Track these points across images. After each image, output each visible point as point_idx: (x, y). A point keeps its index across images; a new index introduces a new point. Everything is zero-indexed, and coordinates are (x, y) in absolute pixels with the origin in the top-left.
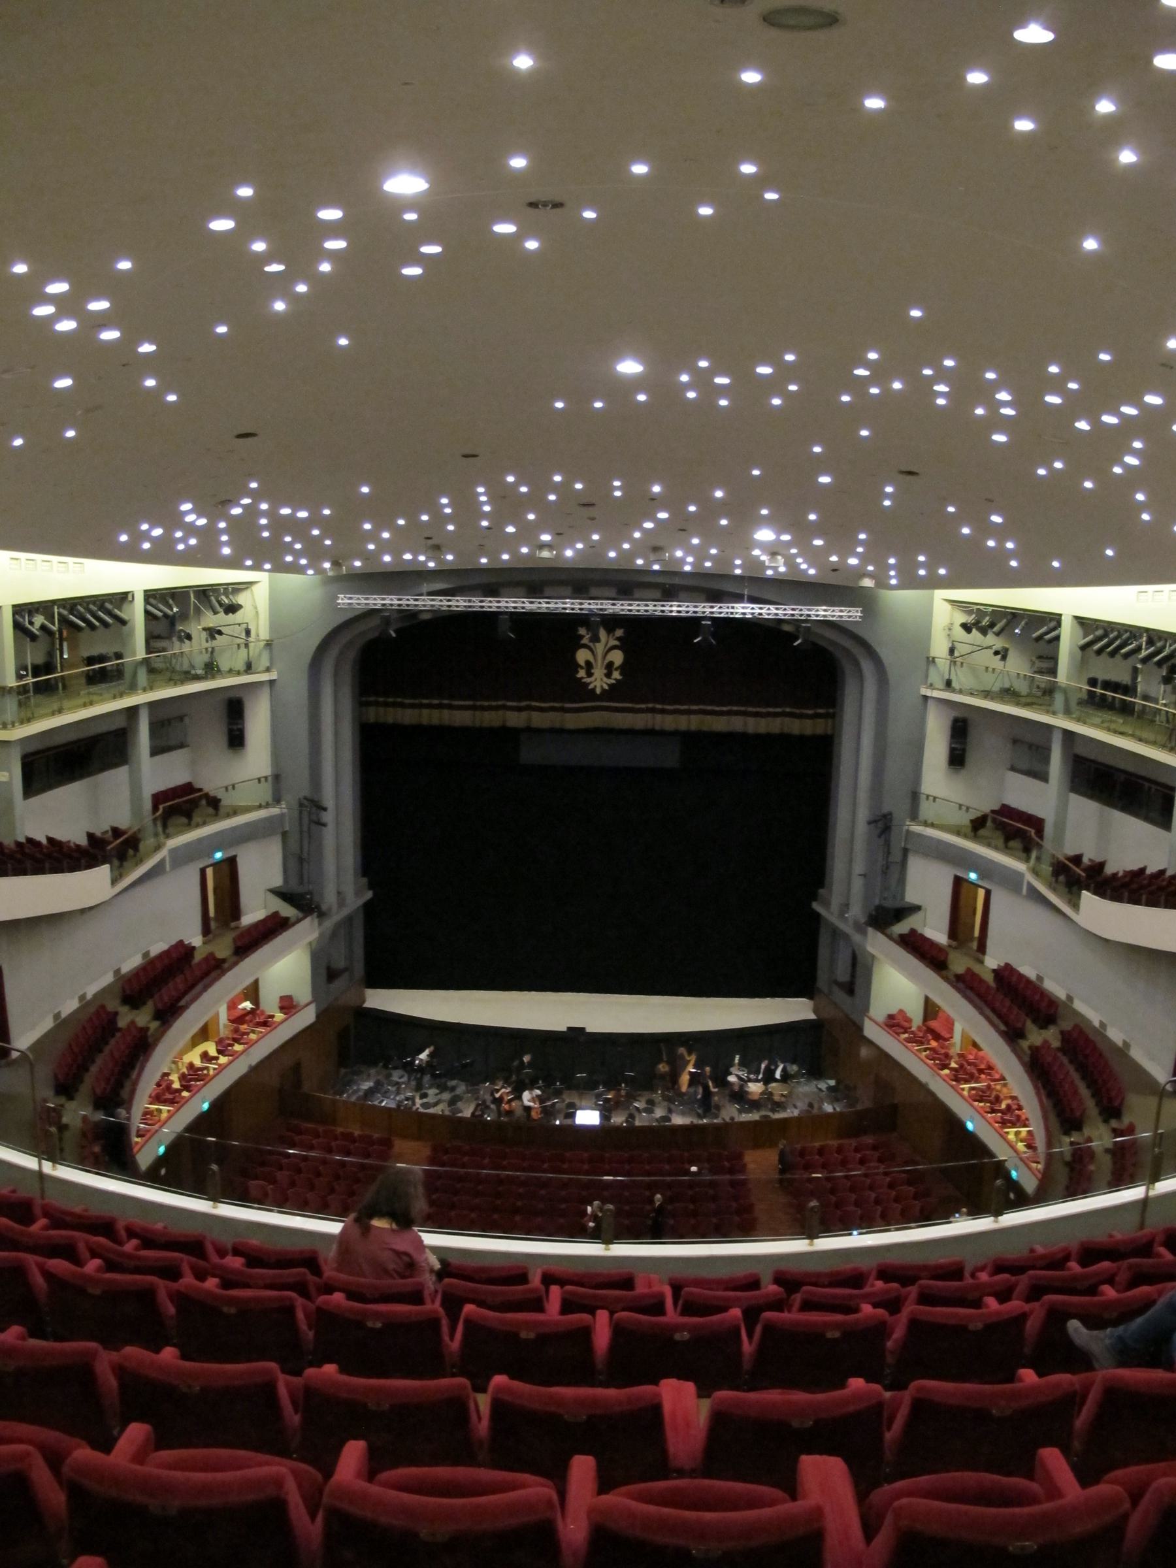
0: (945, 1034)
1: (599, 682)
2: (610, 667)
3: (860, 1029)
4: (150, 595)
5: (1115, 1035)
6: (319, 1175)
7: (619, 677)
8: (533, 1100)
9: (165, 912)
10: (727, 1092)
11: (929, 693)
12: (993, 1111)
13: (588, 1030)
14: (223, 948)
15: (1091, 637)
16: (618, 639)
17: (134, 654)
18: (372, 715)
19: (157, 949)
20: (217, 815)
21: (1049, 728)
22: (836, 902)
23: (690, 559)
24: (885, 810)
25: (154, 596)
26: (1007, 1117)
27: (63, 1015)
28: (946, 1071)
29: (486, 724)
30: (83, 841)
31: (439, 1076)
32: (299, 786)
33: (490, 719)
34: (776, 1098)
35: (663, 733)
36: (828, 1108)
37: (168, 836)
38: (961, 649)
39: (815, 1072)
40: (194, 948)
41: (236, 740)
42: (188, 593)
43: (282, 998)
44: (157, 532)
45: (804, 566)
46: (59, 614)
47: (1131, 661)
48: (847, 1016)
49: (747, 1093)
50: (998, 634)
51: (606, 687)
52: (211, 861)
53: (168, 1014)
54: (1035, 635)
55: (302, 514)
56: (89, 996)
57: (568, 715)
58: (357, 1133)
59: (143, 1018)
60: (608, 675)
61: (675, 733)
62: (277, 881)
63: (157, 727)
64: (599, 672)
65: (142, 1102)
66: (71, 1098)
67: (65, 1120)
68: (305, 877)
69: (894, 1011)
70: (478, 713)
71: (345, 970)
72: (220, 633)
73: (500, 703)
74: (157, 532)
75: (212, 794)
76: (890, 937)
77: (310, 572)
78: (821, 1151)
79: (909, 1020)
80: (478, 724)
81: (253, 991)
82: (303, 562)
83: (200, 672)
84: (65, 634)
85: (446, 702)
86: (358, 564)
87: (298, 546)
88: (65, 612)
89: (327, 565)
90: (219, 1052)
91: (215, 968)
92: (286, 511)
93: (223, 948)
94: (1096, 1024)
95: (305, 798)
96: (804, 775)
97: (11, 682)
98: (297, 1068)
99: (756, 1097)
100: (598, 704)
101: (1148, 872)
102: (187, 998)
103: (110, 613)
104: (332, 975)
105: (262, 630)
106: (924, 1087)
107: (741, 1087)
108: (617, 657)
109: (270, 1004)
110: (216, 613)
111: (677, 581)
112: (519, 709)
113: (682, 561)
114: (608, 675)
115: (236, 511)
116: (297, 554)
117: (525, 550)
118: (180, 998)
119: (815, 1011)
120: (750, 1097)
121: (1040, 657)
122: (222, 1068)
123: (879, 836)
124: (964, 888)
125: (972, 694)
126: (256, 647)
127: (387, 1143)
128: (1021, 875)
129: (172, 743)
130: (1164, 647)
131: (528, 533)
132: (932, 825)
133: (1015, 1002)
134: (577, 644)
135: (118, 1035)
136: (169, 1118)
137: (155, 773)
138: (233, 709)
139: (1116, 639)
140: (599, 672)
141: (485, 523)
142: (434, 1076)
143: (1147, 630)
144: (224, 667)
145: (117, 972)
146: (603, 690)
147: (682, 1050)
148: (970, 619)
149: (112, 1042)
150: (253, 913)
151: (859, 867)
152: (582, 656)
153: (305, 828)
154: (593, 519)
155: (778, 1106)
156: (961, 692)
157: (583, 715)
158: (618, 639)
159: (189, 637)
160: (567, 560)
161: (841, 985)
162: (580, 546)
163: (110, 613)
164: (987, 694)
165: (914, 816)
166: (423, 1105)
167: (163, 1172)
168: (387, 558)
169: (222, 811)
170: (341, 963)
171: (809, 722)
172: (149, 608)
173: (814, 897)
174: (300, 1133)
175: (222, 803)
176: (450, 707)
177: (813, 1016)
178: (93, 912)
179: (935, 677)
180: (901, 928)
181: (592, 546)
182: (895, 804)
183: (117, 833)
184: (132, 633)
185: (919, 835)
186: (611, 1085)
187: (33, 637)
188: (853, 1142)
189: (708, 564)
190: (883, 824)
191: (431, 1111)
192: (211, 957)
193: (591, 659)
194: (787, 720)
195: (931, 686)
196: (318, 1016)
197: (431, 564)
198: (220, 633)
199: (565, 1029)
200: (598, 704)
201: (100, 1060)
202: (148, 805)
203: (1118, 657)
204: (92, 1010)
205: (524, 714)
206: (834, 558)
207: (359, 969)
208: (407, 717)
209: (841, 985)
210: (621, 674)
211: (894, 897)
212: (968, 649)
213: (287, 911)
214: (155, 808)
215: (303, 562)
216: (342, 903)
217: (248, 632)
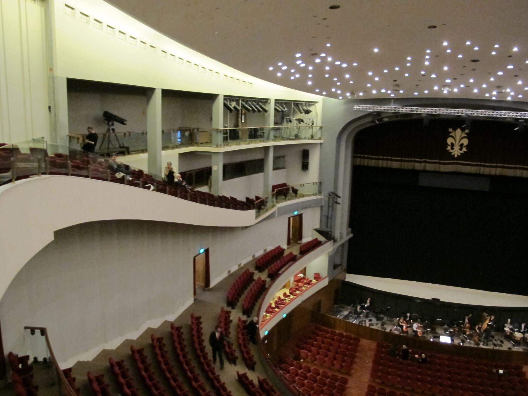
1: (456, 152)
4: (277, 102)
6: (329, 350)
9: (273, 235)
13: (441, 300)
14: (295, 250)
16: (466, 134)
17: (269, 125)
18: (358, 162)
19: (270, 248)
20: (296, 196)
23: (512, 94)
25: (278, 103)
27: (232, 272)
29: (406, 168)
30: (244, 200)
31: (377, 313)
32: (329, 188)
35: (483, 176)
37: (277, 202)
40: (284, 249)
41: (305, 167)
42: (291, 103)
43: (315, 274)
44: (284, 68)
46: (242, 104)
49: (515, 337)
51: (459, 154)
52: (293, 215)
53: (274, 276)
55: (344, 65)
56: (242, 265)
57: (442, 166)
58: (345, 334)
59: (264, 276)
60: (461, 149)
61: (490, 176)
62: (318, 226)
63: (276, 159)
64: (457, 147)
65: (263, 313)
66: (233, 308)
67: (231, 318)
68: (329, 225)
70: (403, 163)
71: (340, 265)
72: (302, 121)
73: (413, 159)
74: (284, 68)
75: (295, 187)
77: (341, 98)
80: (402, 167)
81: (304, 271)
82: (339, 92)
84: (243, 112)
85: (389, 158)
86: (361, 94)
87: (338, 84)
88: (244, 103)
89: (348, 94)
90: (290, 293)
91: (293, 259)
92: (338, 63)
93: (295, 250)
95: (332, 192)
97: (221, 127)
98: (319, 303)
99: (519, 339)
100: (455, 161)
102: (283, 270)
103: (261, 107)
104: (335, 267)
105: (318, 122)
107: (511, 333)
108: (465, 142)
109: (310, 275)
110: (301, 113)
111: (503, 105)
112: (420, 162)
113: (508, 94)
114: (461, 149)
115: (318, 61)
116: (337, 88)
117: (436, 88)
118: (279, 269)
120: (516, 339)
122: (292, 300)
126: (316, 129)
127: (359, 341)
129: (281, 166)
131: (442, 76)
134: (448, 135)
135: (254, 282)
136: (270, 320)
137: (272, 177)
138: (305, 154)
140: (457, 147)
141: (423, 73)
144: (303, 137)
145: (254, 256)
146: (458, 156)
147: (485, 314)
149: (251, 285)
150: (308, 237)
152: (450, 141)
153: (331, 205)
154: (474, 70)
159: (290, 121)
160: (456, 93)
162: (462, 86)
163: (261, 107)
166: (370, 325)
167: (266, 342)
168: (374, 92)
169: (298, 195)
170: (338, 262)
172: (276, 107)
174: (321, 331)
175: (298, 192)
176: (392, 160)
178: (244, 231)
183: (257, 198)
184: (269, 116)
186: (451, 325)
187: (231, 110)
189: (520, 96)
191: (373, 327)
192: (291, 254)
193: (454, 142)
196: (330, 282)
197: (392, 95)
198: (302, 121)
199: (431, 299)
200: (455, 161)
201: (246, 292)
202: (270, 189)
204: (244, 271)
205: (423, 164)
207: (345, 266)
208: (373, 163)
210: (466, 149)
213: (321, 238)
214: (273, 190)
215: (339, 92)
216: (341, 238)
217: (313, 124)
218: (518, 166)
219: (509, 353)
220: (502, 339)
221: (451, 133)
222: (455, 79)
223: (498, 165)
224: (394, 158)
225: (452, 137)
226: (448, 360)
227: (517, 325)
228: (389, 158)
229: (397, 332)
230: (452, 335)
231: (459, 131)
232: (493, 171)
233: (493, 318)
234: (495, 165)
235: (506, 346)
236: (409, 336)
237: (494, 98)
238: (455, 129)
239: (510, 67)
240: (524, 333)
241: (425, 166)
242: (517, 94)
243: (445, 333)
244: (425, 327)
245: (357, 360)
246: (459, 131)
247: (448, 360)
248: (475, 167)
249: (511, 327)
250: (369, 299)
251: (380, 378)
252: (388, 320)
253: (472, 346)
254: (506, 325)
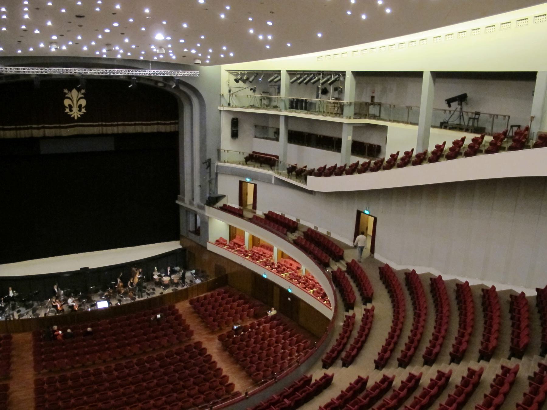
0: (241, 243)
1: (76, 114)
2: (80, 107)
3: (206, 248)
5: (322, 231)
7: (85, 111)
8: (73, 302)
10: (153, 283)
11: (222, 109)
12: (272, 269)
13: (90, 268)
15: (295, 78)
16: (82, 94)
21: (278, 116)
22: (187, 198)
23: (121, 51)
24: (208, 158)
26: (280, 270)
28: (248, 257)
33: (24, 134)
34: (176, 281)
35: (106, 135)
36: (198, 281)
38: (233, 90)
39: (186, 268)
45: (171, 55)
47: (315, 85)
48: (198, 244)
49: (163, 281)
50: (250, 82)
51: (79, 116)
54: (269, 80)
57: (62, 130)
60: (80, 111)
61: (113, 135)
64: (75, 109)
69: (218, 238)
70: (18, 131)
73: (29, 126)
76: (217, 209)
78: (205, 298)
79: (226, 241)
80: (19, 137)
96: (169, 148)
99: (167, 282)
100: (76, 124)
101: (327, 167)
106: (240, 266)
107: (160, 279)
108: (83, 102)
111: (115, 63)
112: (38, 128)
113: (117, 52)
114: (80, 111)
117: (42, 45)
119: (181, 244)
121: (264, 92)
123: (207, 168)
124: (243, 184)
125: (241, 107)
127: (10, 338)
128: (271, 176)
130: (331, 77)
132: (228, 162)
133: (277, 223)
134: (64, 97)
139: (306, 78)
140: (75, 109)
142: (21, 301)
143: (323, 71)
146: (78, 117)
147: (134, 269)
148: (239, 77)
151: (197, 183)
152: (67, 102)
154: (81, 26)
155: (177, 284)
156: (236, 107)
157: (69, 130)
160: (64, 51)
161: (192, 232)
164: (248, 107)
165: (219, 159)
166: (19, 316)
171: (168, 127)
173: (177, 199)
177: (181, 247)
179: (223, 102)
180: (220, 204)
181: (77, 43)
182: (211, 154)
185: (222, 167)
186: (105, 289)
188: (216, 292)
189: (129, 54)
190: (207, 164)
193: (72, 104)
194: (160, 126)
195: (223, 106)
200: (76, 124)
203: (309, 84)
205: (42, 130)
206: (186, 50)
209: (192, 232)
210: (85, 110)
211: (214, 193)
212: (238, 89)
218: (137, 122)
219: (162, 297)
220: (154, 287)
221: (67, 94)
222: (62, 35)
223: (120, 123)
224: (6, 127)
226: (110, 323)
227: (163, 270)
229: (51, 314)
230: (108, 299)
231: (74, 92)
232: (115, 130)
233: (141, 270)
234: (116, 123)
235: (158, 292)
236: (66, 313)
237: (105, 56)
238: (70, 90)
239: (116, 25)
240: (170, 276)
241: (44, 133)
242: (126, 52)
243: (101, 298)
244: (79, 300)
245: (14, 359)
246: (74, 92)
247: (110, 323)
248: (98, 128)
249: (158, 274)
250: (10, 288)
251: (45, 367)
252: (38, 305)
253: (129, 302)
254: (154, 273)
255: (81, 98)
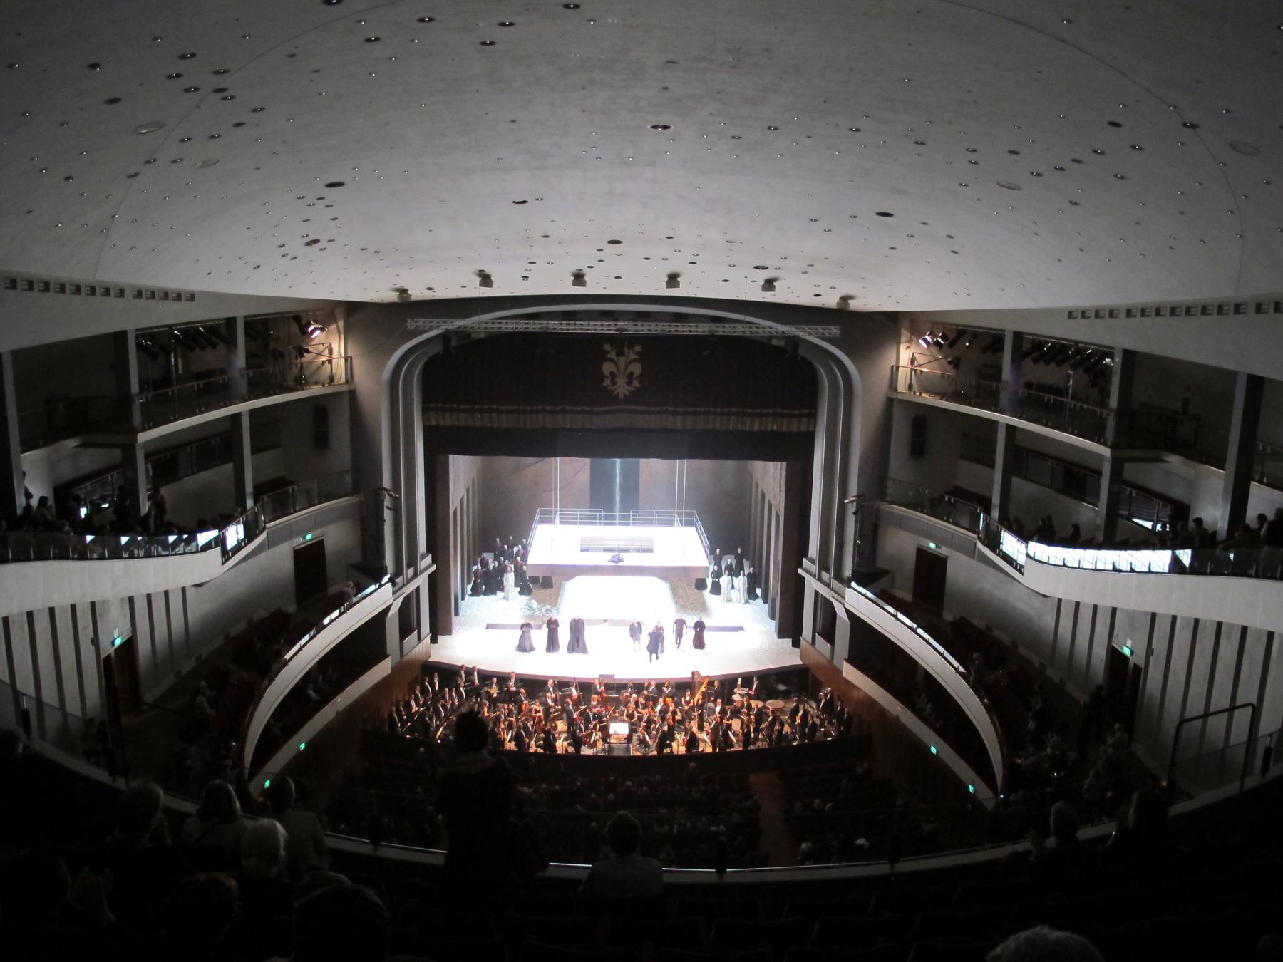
1: (622, 388)
16: (637, 353)
21: (993, 424)
40: (290, 615)
41: (322, 441)
60: (629, 384)
64: (621, 381)
83: (291, 384)
85: (494, 407)
94: (1037, 664)
108: (637, 369)
134: (603, 358)
140: (621, 381)
152: (607, 368)
158: (637, 353)
196: (393, 669)
225: (611, 360)
228: (494, 407)
255: (635, 360)
